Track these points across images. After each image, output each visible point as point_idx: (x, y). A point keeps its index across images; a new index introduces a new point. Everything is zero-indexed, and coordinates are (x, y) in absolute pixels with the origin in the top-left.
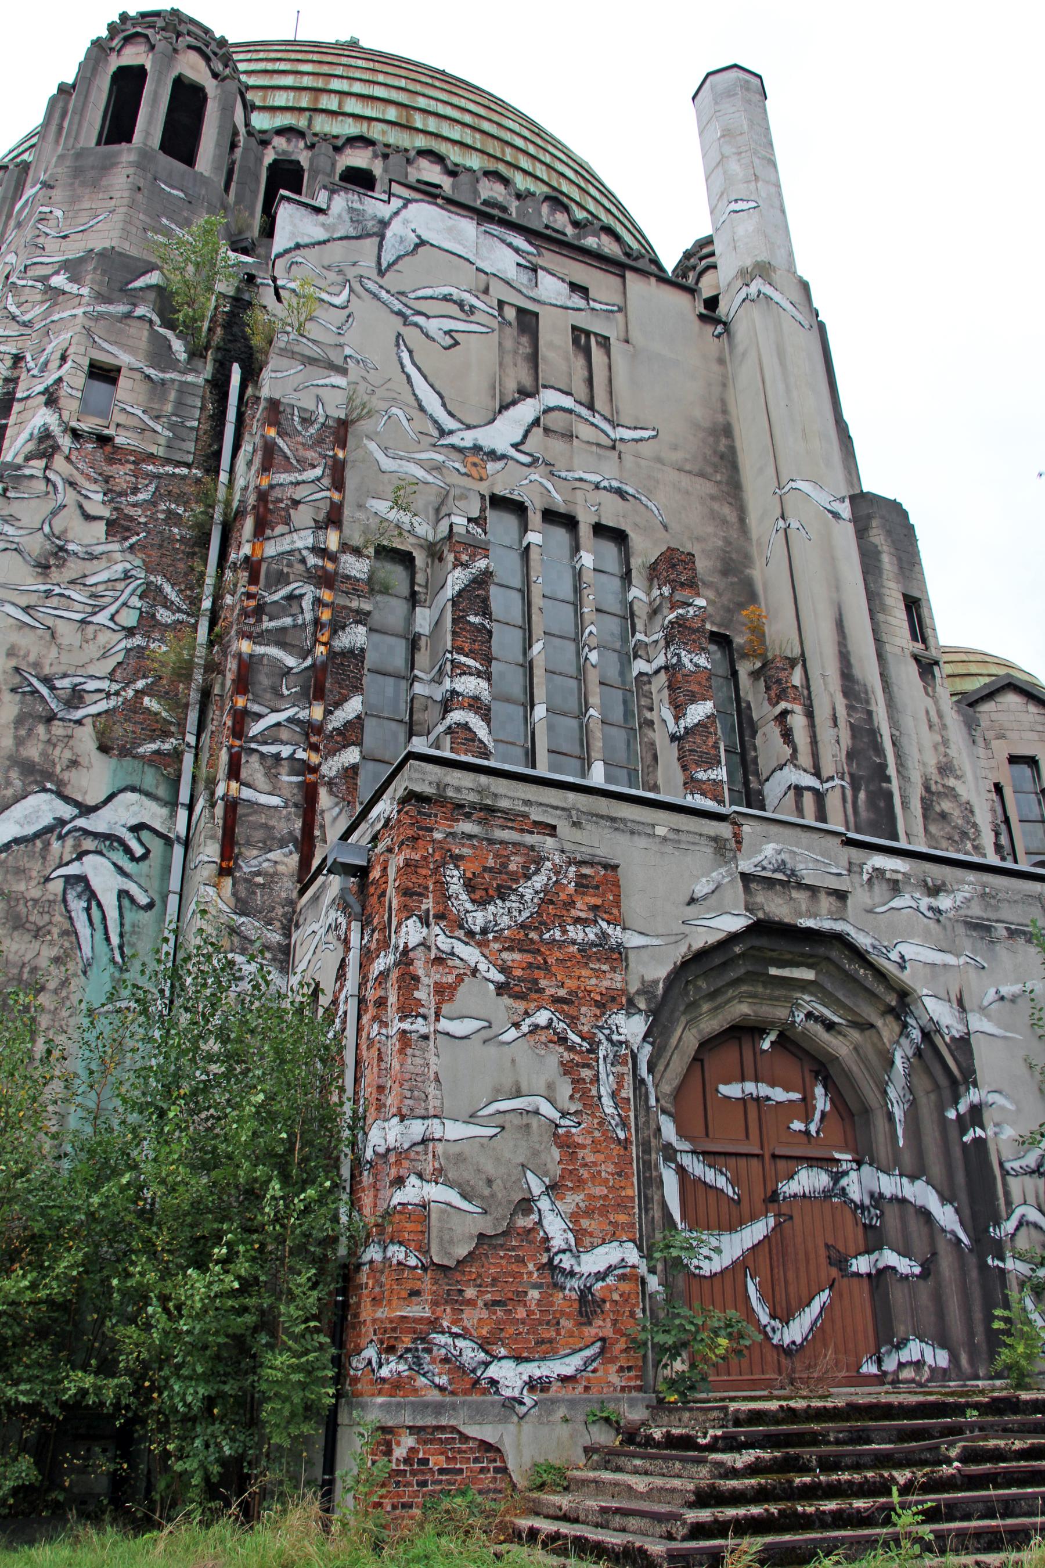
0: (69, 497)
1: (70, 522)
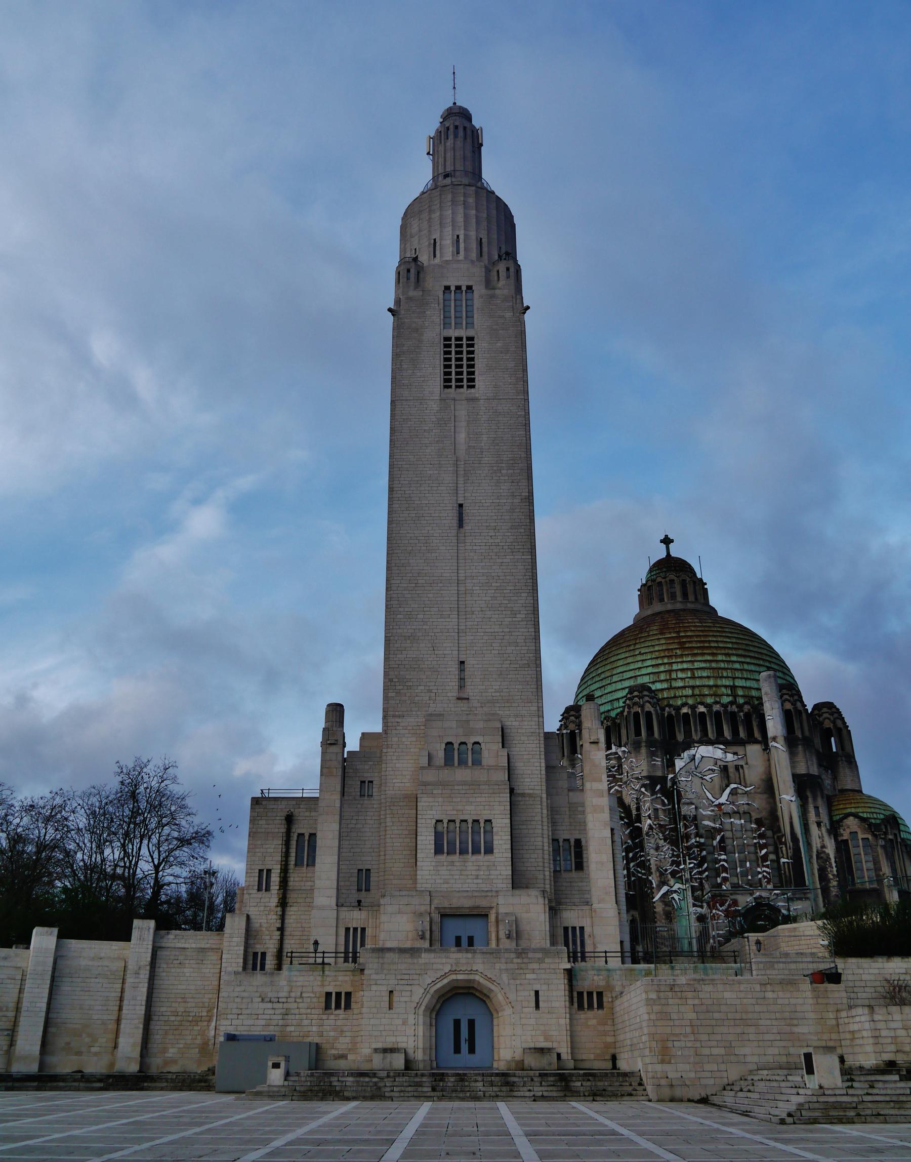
1: (658, 840)
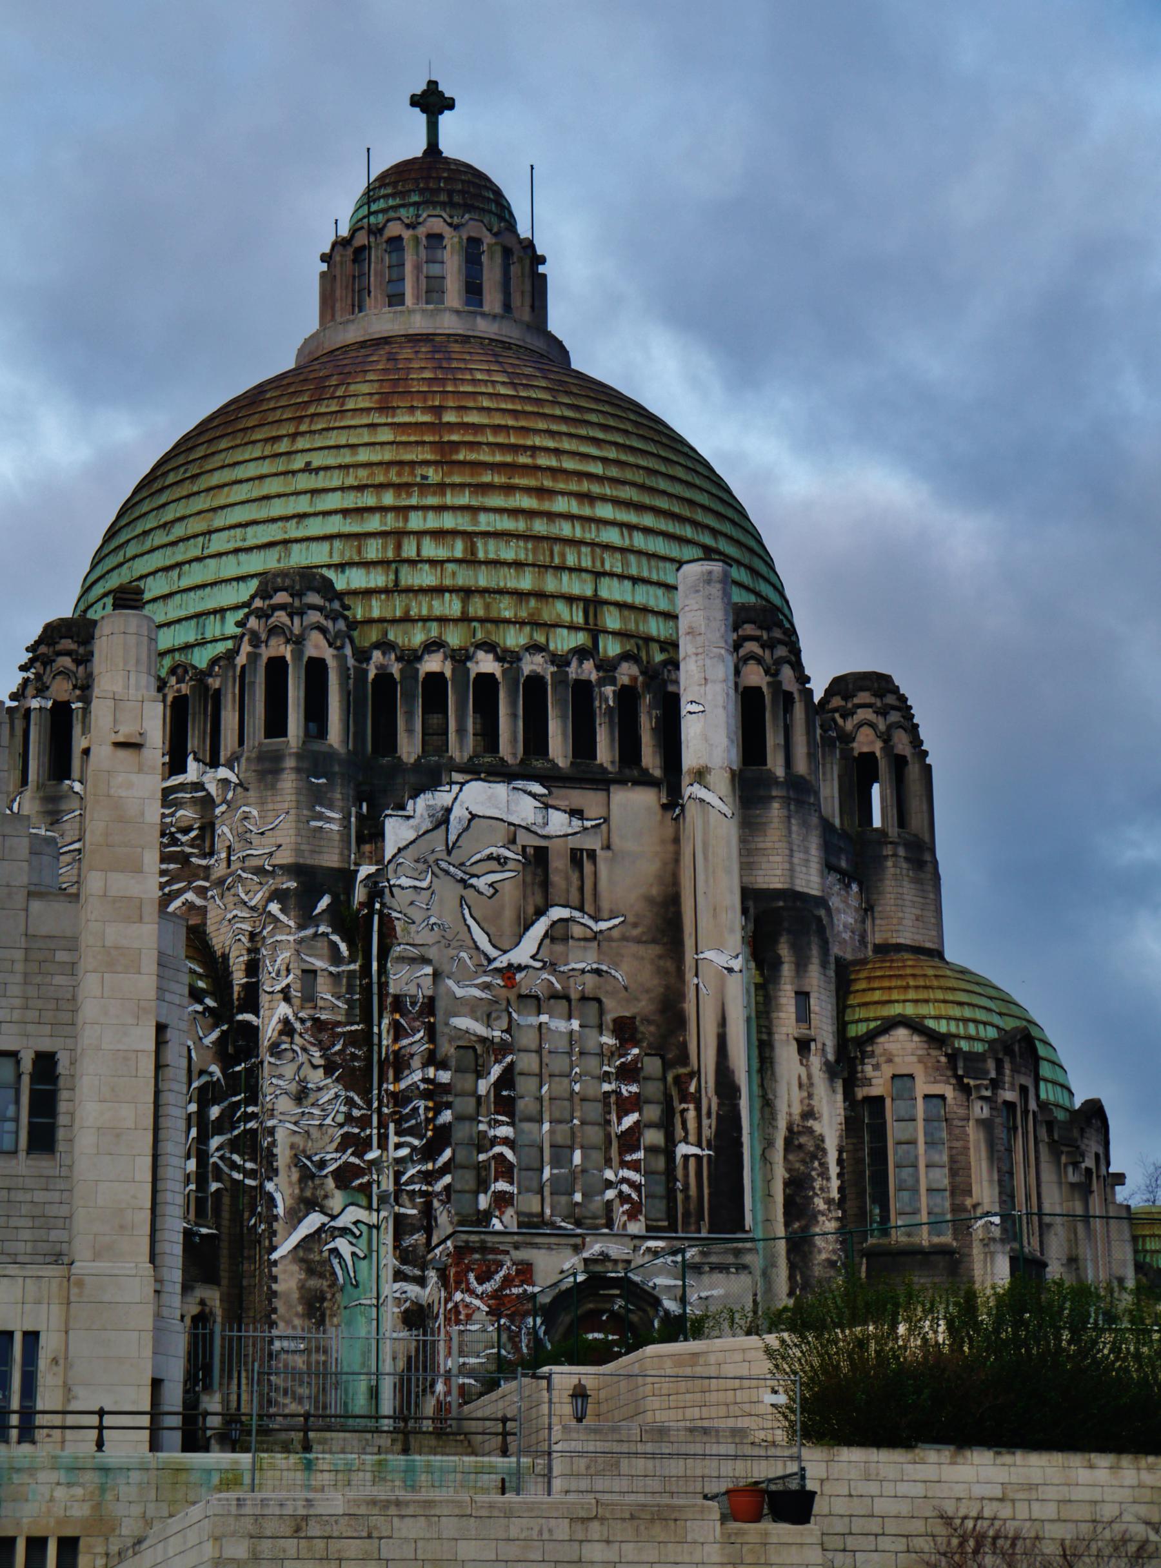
0: (302, 1057)
1: (307, 1070)
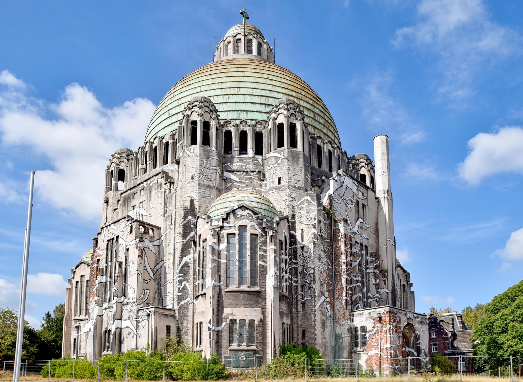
1: (320, 251)
